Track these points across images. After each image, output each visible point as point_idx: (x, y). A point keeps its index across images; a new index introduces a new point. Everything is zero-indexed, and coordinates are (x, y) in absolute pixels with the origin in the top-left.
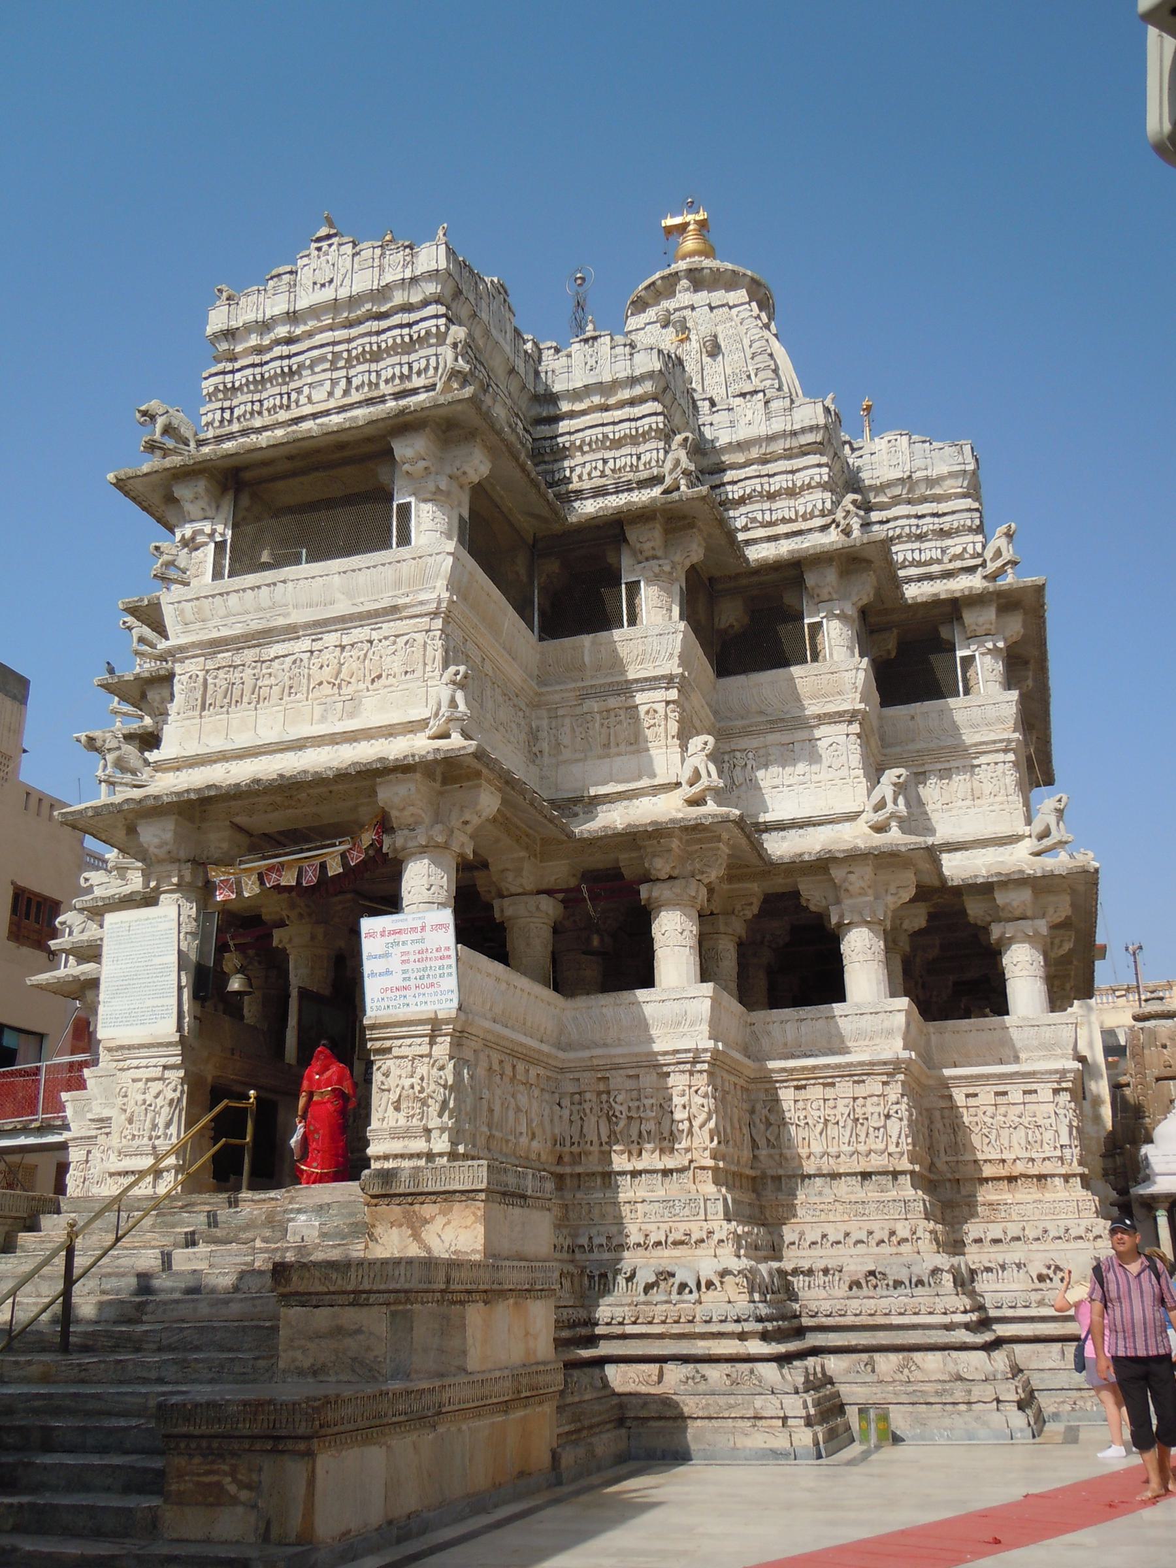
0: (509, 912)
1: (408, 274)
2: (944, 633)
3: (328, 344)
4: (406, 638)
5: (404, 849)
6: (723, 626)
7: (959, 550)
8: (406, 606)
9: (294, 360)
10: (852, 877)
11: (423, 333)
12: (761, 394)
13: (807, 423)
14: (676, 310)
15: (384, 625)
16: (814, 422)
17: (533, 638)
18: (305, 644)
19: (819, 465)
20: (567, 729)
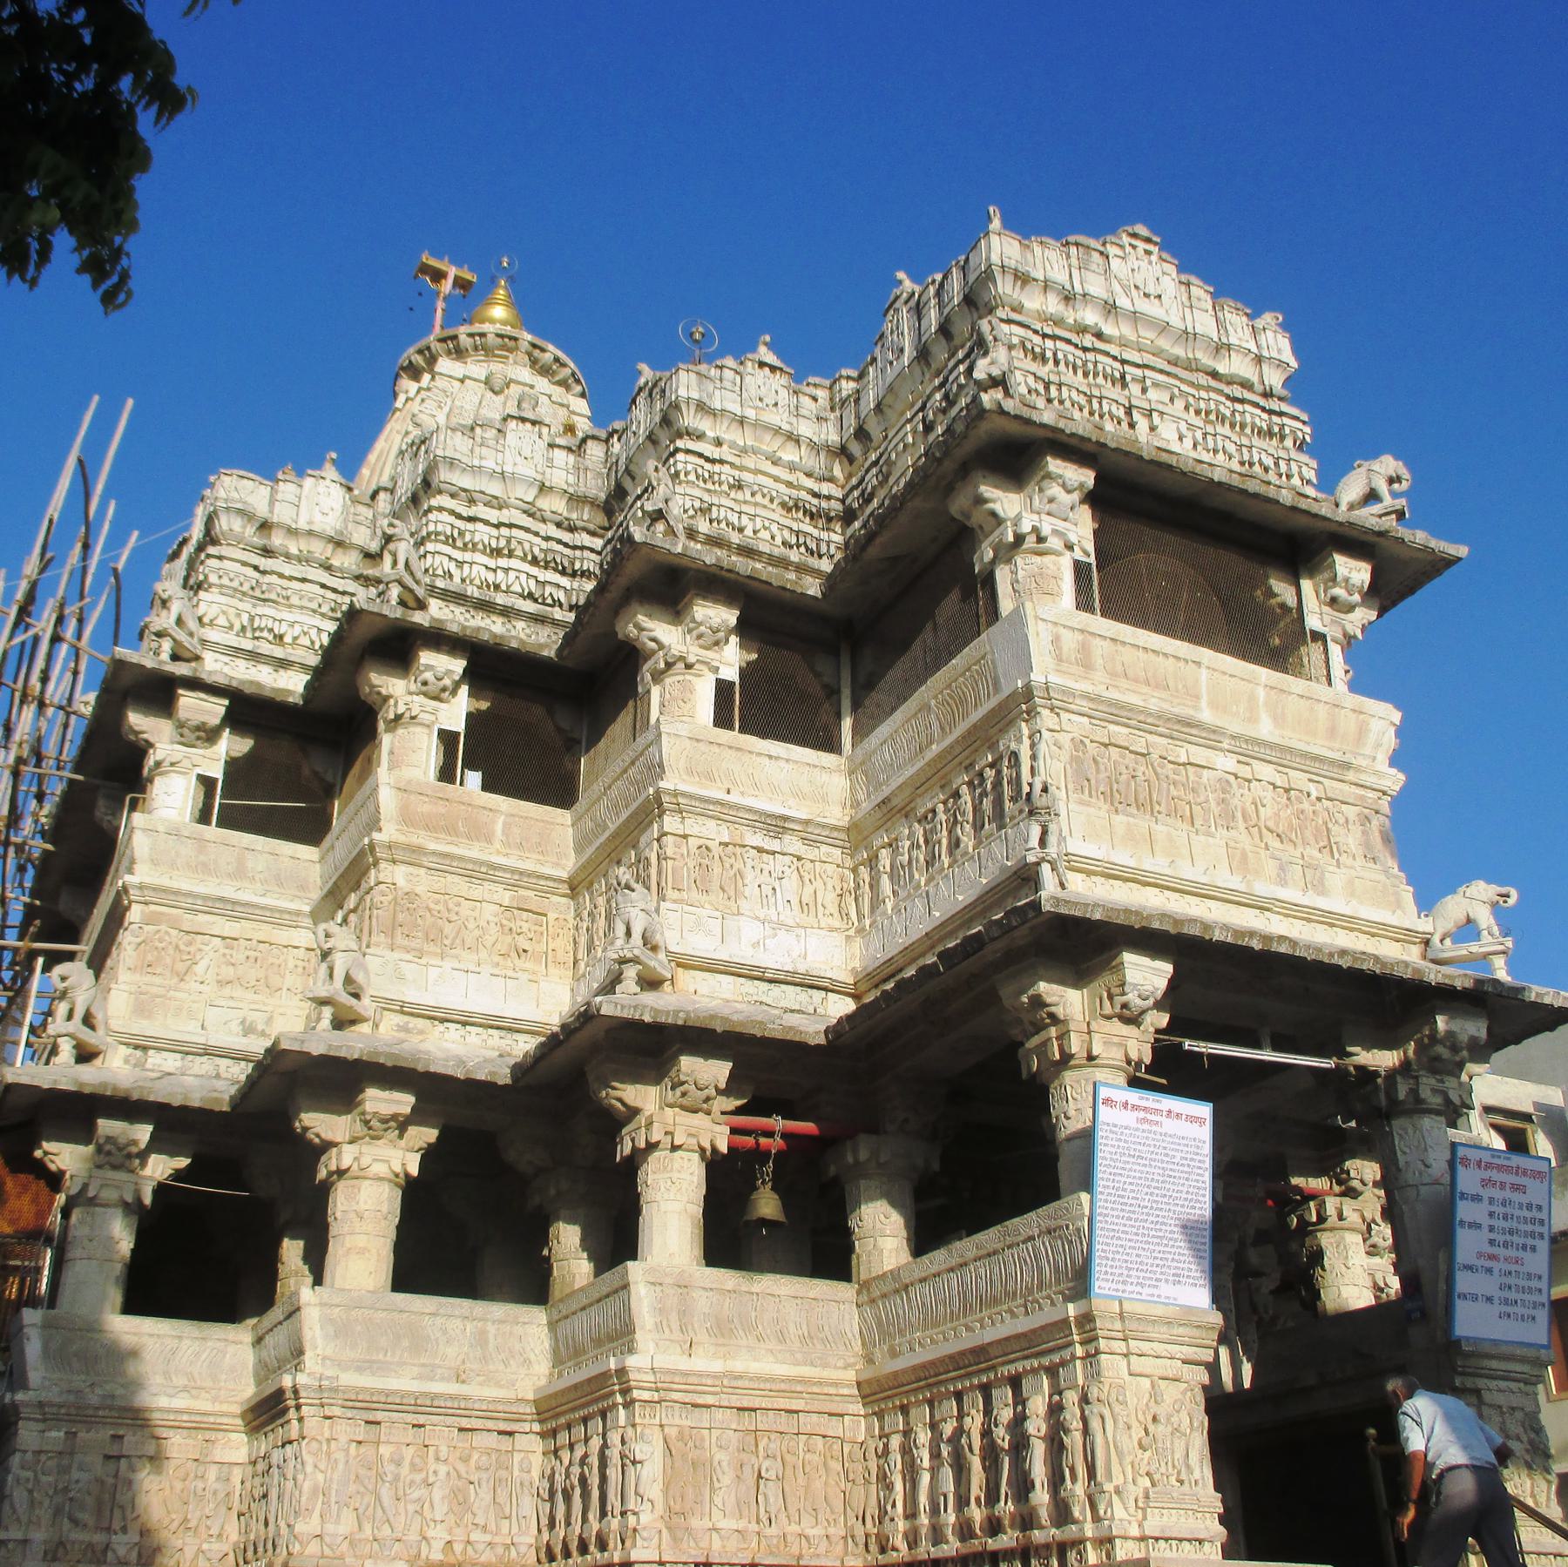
8: (1358, 769)
9: (1128, 368)
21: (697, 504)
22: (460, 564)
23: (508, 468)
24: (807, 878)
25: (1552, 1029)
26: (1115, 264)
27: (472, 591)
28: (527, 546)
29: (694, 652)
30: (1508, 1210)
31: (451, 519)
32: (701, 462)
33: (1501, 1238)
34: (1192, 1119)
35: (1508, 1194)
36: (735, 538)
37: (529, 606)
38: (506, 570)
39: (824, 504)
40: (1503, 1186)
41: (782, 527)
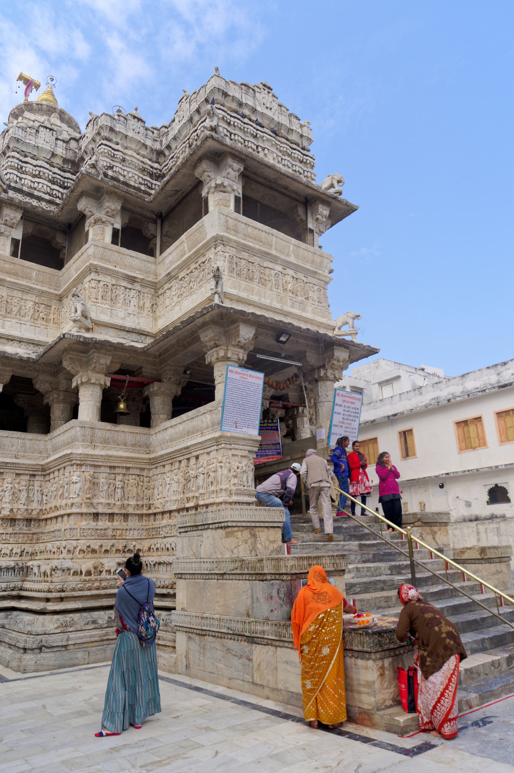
8: (320, 274)
15: (309, 277)
18: (279, 268)
21: (108, 164)
22: (21, 179)
23: (40, 145)
24: (142, 298)
25: (367, 357)
26: (257, 94)
27: (25, 189)
28: (46, 175)
29: (104, 218)
31: (17, 161)
32: (110, 149)
33: (346, 417)
34: (258, 378)
35: (349, 405)
36: (122, 178)
37: (47, 197)
38: (39, 183)
39: (155, 171)
40: (348, 402)
41: (139, 177)
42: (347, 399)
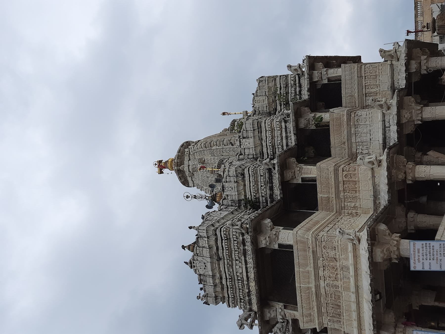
0: (412, 227)
1: (206, 239)
2: (319, 87)
3: (224, 266)
4: (323, 249)
5: (397, 256)
6: (313, 155)
7: (292, 82)
8: (313, 248)
9: (228, 277)
10: (406, 116)
11: (225, 236)
12: (241, 140)
13: (251, 126)
14: (189, 171)
15: (318, 255)
16: (251, 124)
17: (317, 213)
18: (322, 282)
19: (265, 123)
20: (349, 204)
30: (424, 254)
40: (419, 256)
42: (417, 258)
